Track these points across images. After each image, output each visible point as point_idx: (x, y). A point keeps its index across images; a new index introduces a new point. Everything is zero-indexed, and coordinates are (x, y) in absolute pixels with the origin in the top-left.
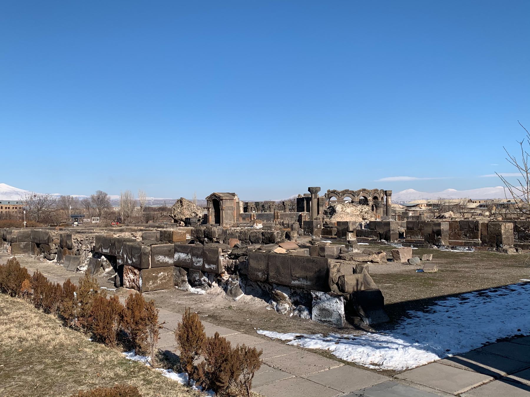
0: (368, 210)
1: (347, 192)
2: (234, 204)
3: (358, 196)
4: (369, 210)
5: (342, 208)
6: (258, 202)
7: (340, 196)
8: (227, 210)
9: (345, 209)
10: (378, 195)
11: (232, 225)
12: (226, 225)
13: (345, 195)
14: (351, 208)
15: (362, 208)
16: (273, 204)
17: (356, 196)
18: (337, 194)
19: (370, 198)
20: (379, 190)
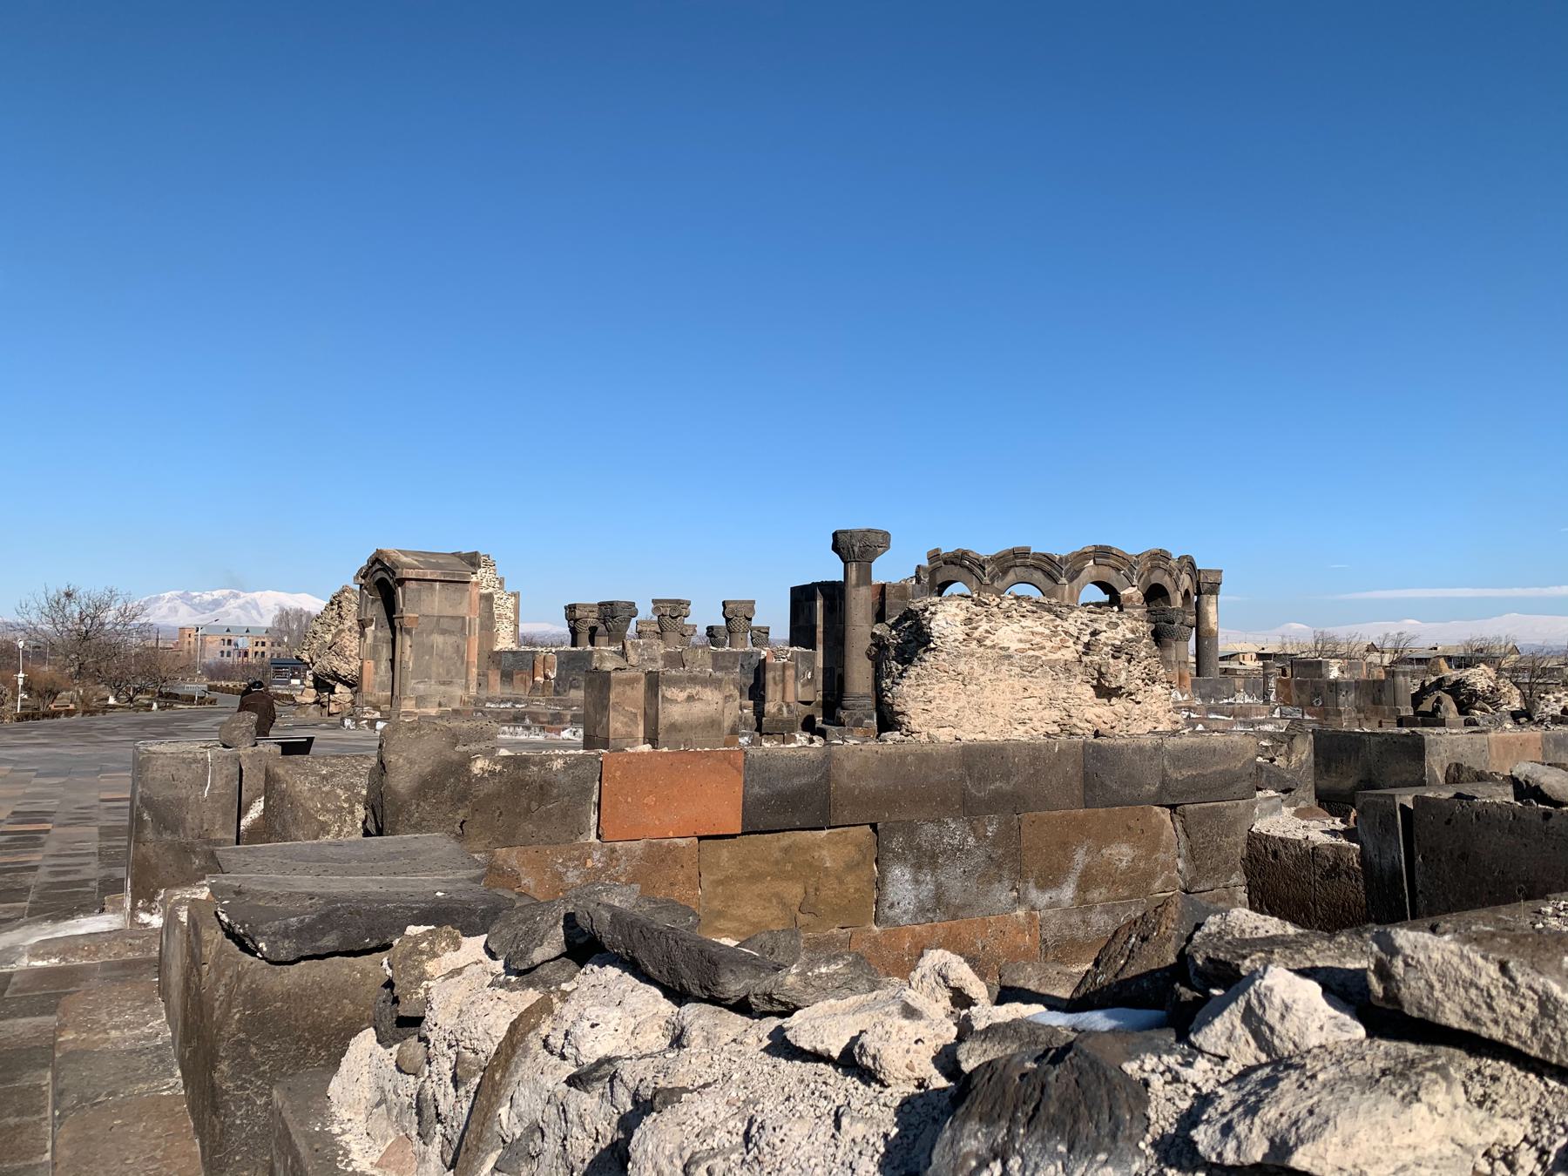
0: (1130, 636)
1: (1018, 561)
2: (470, 604)
3: (1071, 580)
4: (1138, 640)
5: (968, 621)
6: (611, 604)
7: (986, 580)
8: (432, 632)
9: (984, 626)
10: (1167, 578)
11: (457, 706)
12: (417, 706)
13: (1011, 576)
14: (1028, 622)
15: (1096, 626)
16: (674, 609)
17: (1063, 580)
18: (971, 571)
19: (1131, 592)
20: (1175, 556)
